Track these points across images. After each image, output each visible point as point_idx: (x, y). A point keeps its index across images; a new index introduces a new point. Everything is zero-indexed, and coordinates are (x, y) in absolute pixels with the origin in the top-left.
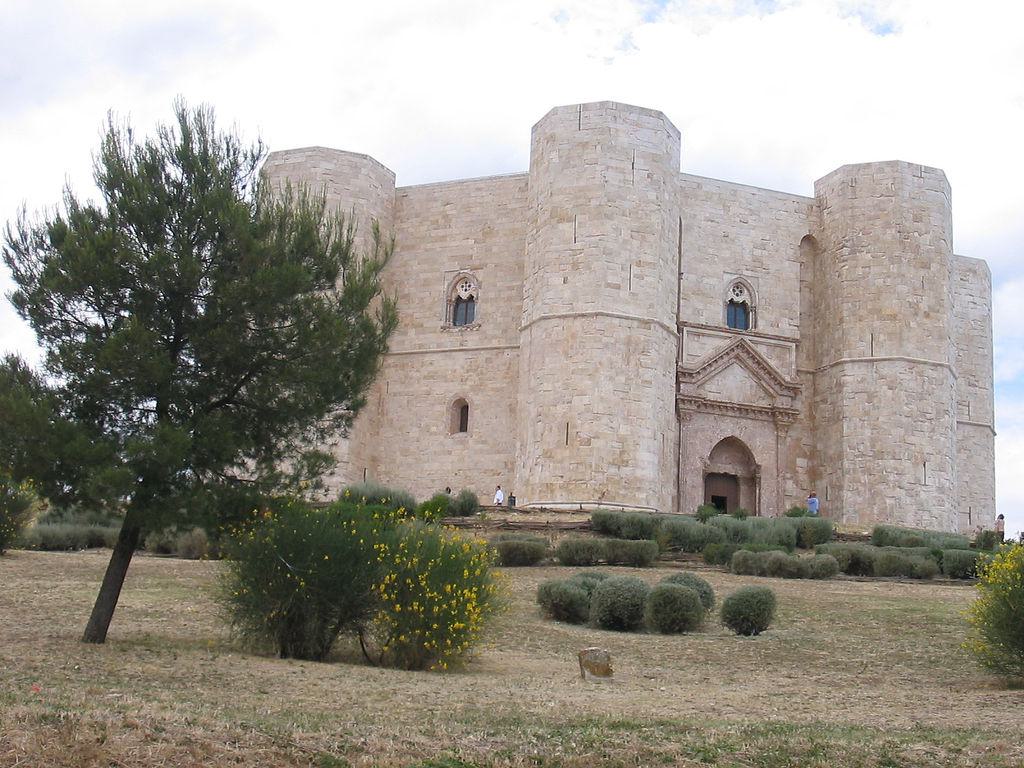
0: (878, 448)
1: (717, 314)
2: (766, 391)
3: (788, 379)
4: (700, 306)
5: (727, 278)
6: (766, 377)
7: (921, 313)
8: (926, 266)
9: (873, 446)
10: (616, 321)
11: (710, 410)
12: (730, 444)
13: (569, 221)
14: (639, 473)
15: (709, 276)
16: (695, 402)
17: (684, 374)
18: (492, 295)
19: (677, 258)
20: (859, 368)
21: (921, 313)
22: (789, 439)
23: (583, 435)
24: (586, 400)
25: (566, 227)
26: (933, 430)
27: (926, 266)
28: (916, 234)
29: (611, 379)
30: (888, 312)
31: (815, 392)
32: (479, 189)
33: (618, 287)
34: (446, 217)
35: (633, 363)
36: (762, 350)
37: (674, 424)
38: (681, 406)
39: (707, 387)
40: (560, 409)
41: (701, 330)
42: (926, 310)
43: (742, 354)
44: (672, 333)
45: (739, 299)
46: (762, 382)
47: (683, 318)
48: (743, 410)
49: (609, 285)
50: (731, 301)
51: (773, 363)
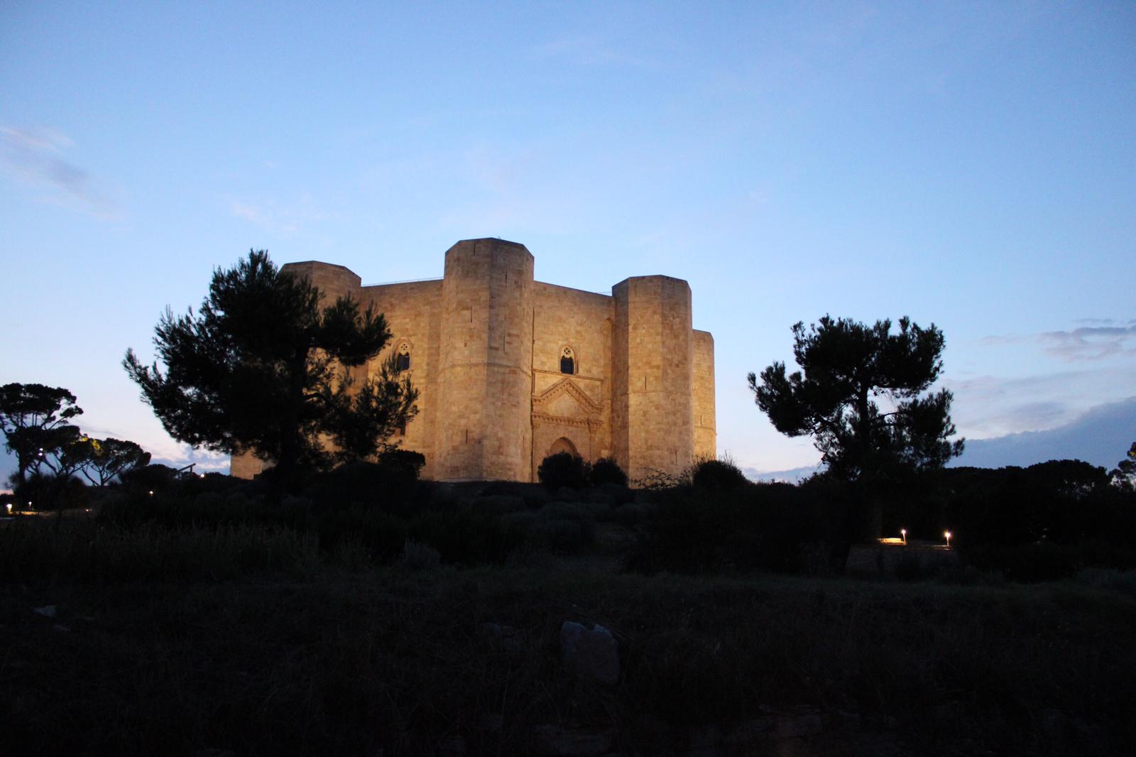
0: (649, 443)
1: (557, 365)
2: (583, 409)
3: (596, 403)
4: (545, 360)
5: (560, 343)
6: (584, 401)
7: (674, 365)
8: (676, 337)
9: (646, 442)
11: (551, 421)
13: (468, 309)
14: (509, 460)
15: (549, 342)
16: (542, 417)
17: (536, 400)
18: (420, 352)
19: (531, 332)
20: (639, 396)
21: (674, 365)
22: (597, 439)
23: (476, 437)
24: (478, 416)
25: (467, 313)
26: (681, 433)
27: (676, 337)
28: (671, 318)
29: (493, 404)
30: (655, 364)
31: (613, 411)
32: (412, 289)
33: (497, 349)
34: (392, 305)
35: (506, 394)
37: (530, 431)
38: (533, 418)
40: (463, 422)
42: (677, 362)
44: (529, 376)
45: (568, 356)
46: (582, 406)
47: (535, 367)
48: (570, 421)
49: (491, 348)
50: (563, 357)
51: (588, 393)
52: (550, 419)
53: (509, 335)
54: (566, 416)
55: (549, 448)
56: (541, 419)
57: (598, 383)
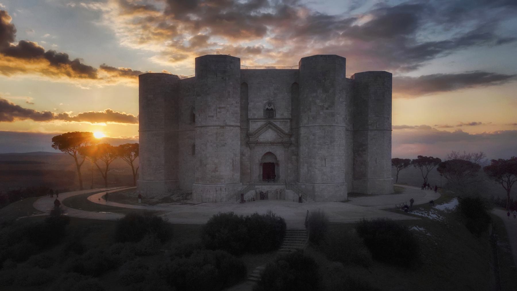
1: (261, 113)
3: (287, 132)
5: (265, 102)
10: (212, 127)
12: (269, 153)
26: (329, 148)
33: (213, 117)
36: (278, 124)
39: (260, 137)
41: (255, 120)
43: (270, 125)
47: (249, 117)
48: (272, 143)
49: (209, 116)
51: (281, 127)
52: (258, 143)
53: (220, 108)
54: (270, 140)
55: (260, 158)
56: (254, 145)
57: (289, 121)
